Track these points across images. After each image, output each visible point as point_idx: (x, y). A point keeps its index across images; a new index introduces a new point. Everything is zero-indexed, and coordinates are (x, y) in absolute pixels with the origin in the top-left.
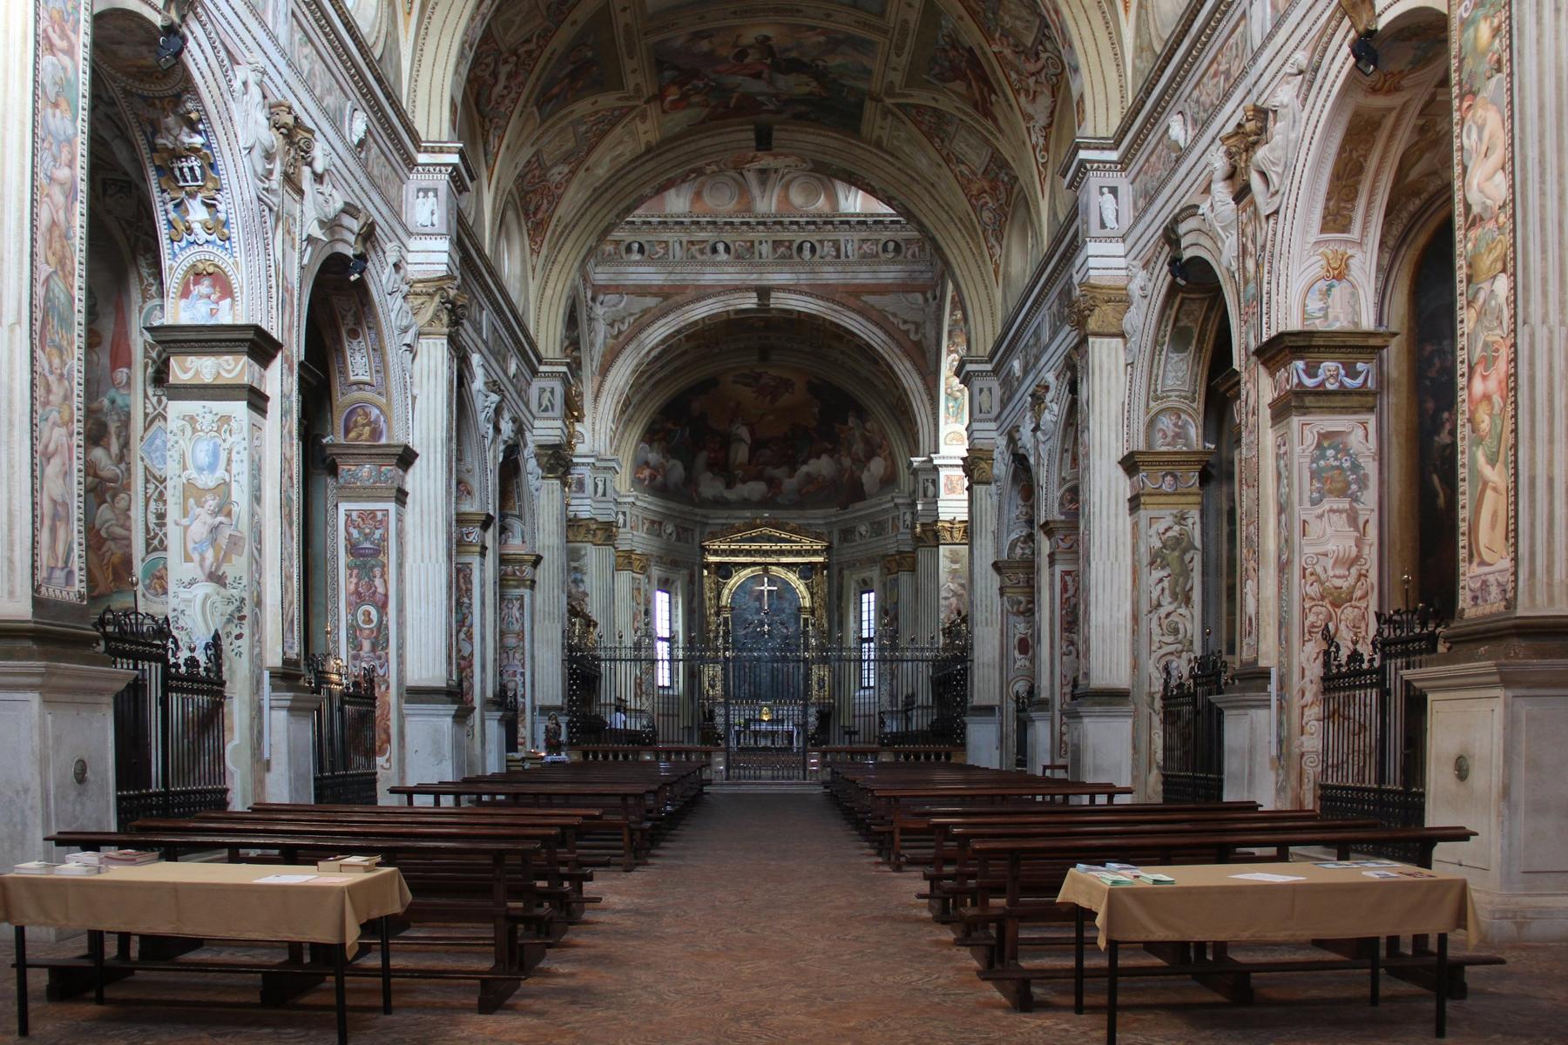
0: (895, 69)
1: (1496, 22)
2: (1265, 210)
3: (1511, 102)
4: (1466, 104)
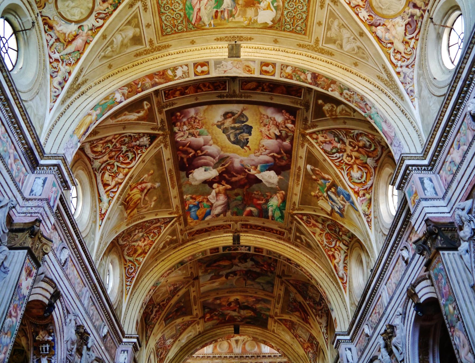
0: (277, 308)
1: (453, 306)
2: (400, 359)
3: (466, 330)
4: (452, 330)
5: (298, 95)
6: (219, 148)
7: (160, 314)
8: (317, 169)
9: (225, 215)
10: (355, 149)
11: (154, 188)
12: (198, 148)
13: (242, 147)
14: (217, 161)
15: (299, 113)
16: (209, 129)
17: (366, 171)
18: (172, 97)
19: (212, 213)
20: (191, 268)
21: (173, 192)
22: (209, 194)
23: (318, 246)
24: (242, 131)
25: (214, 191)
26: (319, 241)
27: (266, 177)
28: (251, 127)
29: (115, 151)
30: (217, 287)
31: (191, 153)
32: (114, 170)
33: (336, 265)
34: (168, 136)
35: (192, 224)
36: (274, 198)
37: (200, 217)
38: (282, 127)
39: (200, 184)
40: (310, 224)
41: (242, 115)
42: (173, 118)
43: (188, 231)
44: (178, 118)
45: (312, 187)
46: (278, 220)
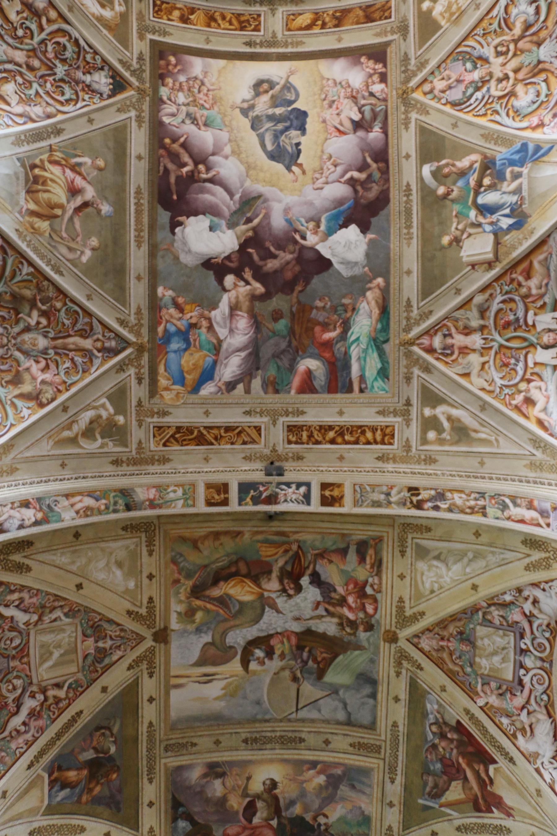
5: (386, 14)
6: (242, 168)
7: (42, 730)
8: (444, 162)
9: (248, 391)
10: (511, 54)
11: (99, 211)
12: (201, 159)
13: (289, 169)
14: (238, 206)
15: (391, 52)
16: (225, 115)
17: (543, 76)
18: (165, 17)
19: (217, 378)
20: (150, 577)
21: (137, 259)
22: (214, 306)
23: (484, 406)
24: (288, 124)
25: (225, 298)
26: (483, 389)
27: (339, 249)
28: (305, 114)
29: (41, 60)
30: (219, 706)
31: (185, 165)
32: (28, 92)
33: (542, 416)
34: (148, 98)
35: (168, 396)
36: (361, 312)
37: (190, 378)
38: (364, 98)
39: (196, 267)
40: (452, 354)
41: (288, 87)
42: (162, 63)
43: (155, 419)
44: (170, 68)
45: (441, 223)
46: (376, 384)
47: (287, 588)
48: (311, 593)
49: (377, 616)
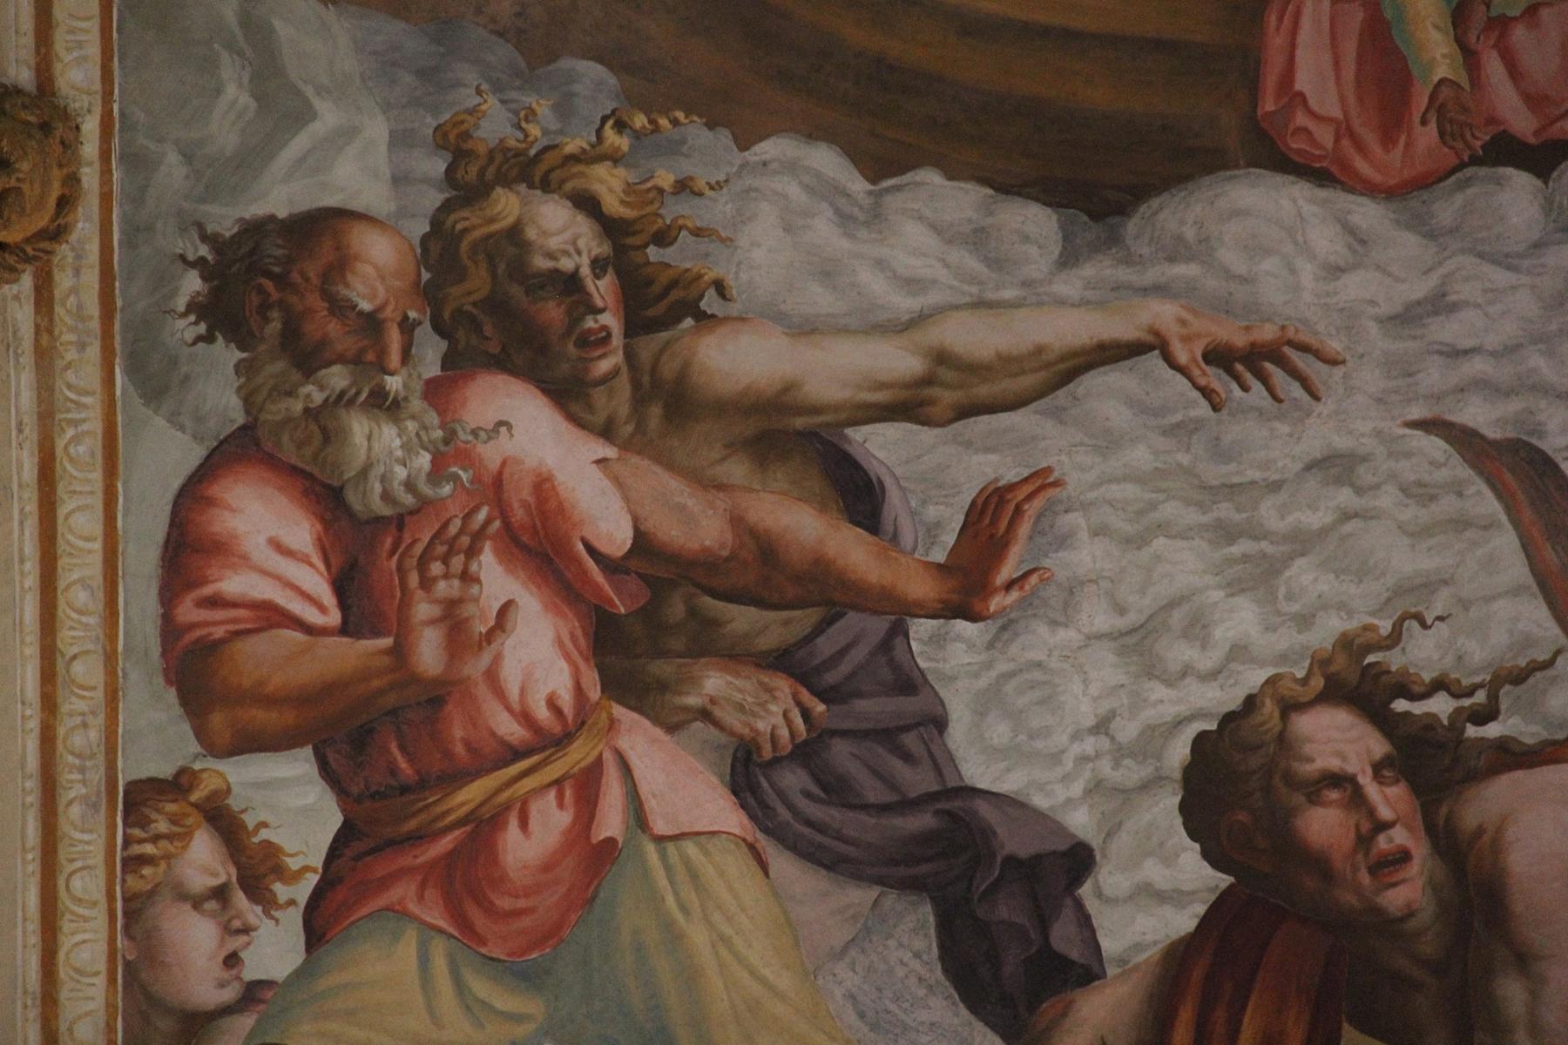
47: (1388, 799)
48: (1066, 720)
49: (165, 455)
